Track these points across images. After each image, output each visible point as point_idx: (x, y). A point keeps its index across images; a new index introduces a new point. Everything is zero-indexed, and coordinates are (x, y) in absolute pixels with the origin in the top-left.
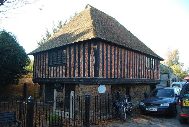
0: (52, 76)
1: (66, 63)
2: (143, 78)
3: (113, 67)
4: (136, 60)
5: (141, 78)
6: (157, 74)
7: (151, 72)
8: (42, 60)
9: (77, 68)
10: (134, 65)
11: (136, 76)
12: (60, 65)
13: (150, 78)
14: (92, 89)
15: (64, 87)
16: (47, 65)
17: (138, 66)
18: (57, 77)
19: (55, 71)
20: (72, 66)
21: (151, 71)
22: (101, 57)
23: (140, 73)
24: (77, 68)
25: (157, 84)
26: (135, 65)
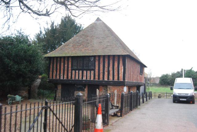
0: (77, 78)
1: (95, 69)
8: (62, 64)
9: (106, 73)
12: (87, 70)
16: (70, 69)
18: (84, 79)
20: (101, 71)
24: (106, 73)
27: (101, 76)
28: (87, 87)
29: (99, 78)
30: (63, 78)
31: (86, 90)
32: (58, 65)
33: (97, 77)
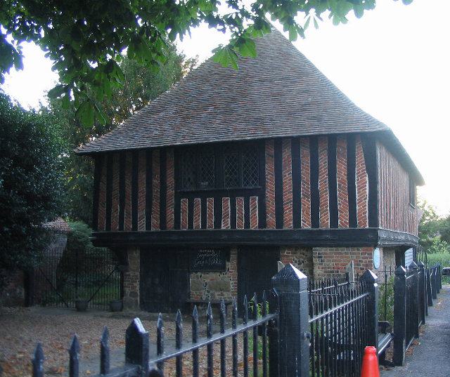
0: (198, 224)
8: (143, 176)
9: (306, 204)
12: (233, 195)
16: (171, 192)
18: (223, 228)
20: (288, 196)
24: (306, 204)
27: (288, 215)
28: (234, 256)
29: (280, 221)
30: (148, 226)
31: (231, 265)
32: (128, 182)
33: (271, 219)
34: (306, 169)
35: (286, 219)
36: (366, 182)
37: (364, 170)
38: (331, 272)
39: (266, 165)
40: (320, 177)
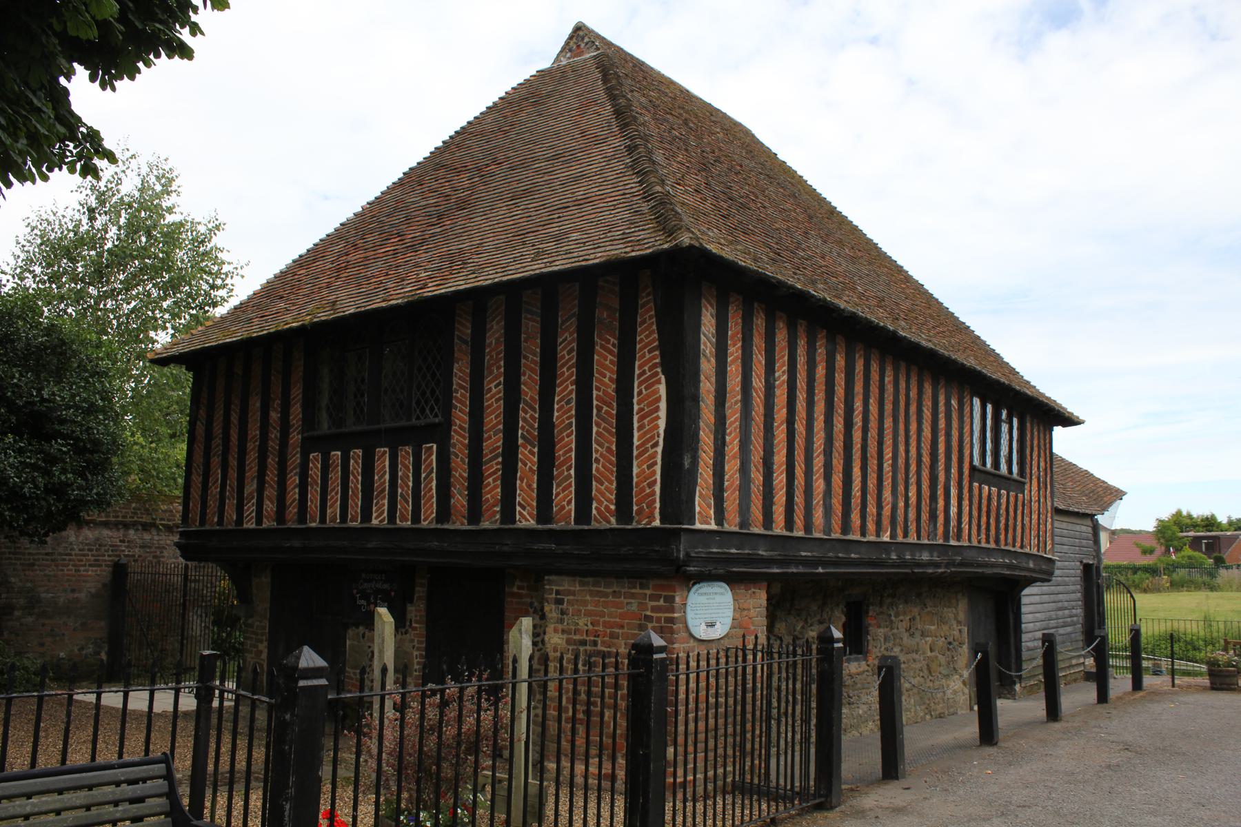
0: (334, 510)
1: (448, 423)
2: (953, 543)
3: (780, 458)
4: (913, 418)
5: (946, 538)
6: (1035, 517)
7: (1004, 500)
8: (256, 404)
9: (528, 458)
10: (902, 448)
11: (912, 527)
12: (395, 439)
13: (997, 541)
14: (642, 606)
15: (420, 591)
16: (295, 438)
17: (926, 459)
18: (375, 522)
19: (356, 482)
20: (493, 441)
21: (999, 496)
22: (707, 387)
23: (941, 503)
24: (528, 458)
25: (1029, 582)
26: (907, 451)
34: (532, 370)
35: (487, 500)
36: (659, 399)
37: (655, 366)
38: (583, 643)
39: (456, 365)
40: (558, 390)
